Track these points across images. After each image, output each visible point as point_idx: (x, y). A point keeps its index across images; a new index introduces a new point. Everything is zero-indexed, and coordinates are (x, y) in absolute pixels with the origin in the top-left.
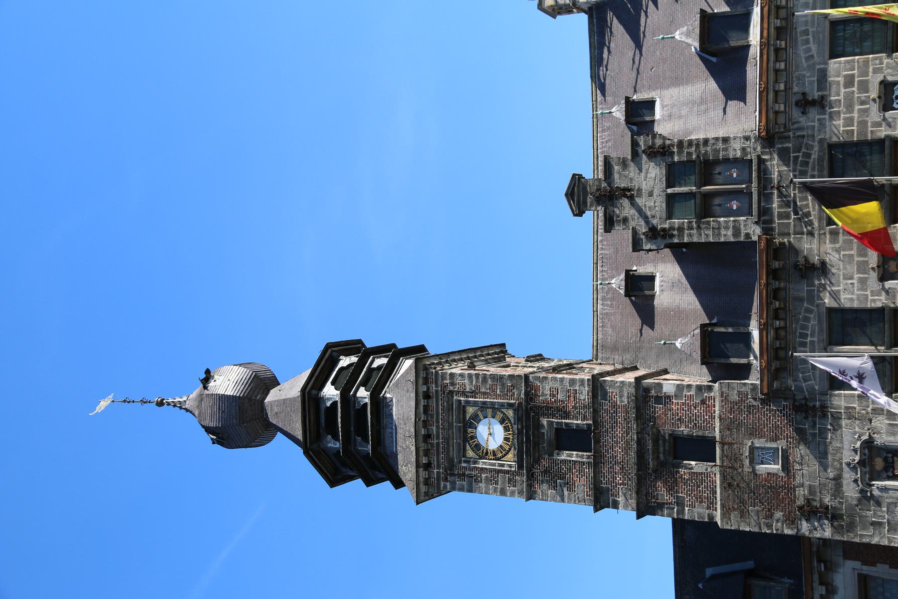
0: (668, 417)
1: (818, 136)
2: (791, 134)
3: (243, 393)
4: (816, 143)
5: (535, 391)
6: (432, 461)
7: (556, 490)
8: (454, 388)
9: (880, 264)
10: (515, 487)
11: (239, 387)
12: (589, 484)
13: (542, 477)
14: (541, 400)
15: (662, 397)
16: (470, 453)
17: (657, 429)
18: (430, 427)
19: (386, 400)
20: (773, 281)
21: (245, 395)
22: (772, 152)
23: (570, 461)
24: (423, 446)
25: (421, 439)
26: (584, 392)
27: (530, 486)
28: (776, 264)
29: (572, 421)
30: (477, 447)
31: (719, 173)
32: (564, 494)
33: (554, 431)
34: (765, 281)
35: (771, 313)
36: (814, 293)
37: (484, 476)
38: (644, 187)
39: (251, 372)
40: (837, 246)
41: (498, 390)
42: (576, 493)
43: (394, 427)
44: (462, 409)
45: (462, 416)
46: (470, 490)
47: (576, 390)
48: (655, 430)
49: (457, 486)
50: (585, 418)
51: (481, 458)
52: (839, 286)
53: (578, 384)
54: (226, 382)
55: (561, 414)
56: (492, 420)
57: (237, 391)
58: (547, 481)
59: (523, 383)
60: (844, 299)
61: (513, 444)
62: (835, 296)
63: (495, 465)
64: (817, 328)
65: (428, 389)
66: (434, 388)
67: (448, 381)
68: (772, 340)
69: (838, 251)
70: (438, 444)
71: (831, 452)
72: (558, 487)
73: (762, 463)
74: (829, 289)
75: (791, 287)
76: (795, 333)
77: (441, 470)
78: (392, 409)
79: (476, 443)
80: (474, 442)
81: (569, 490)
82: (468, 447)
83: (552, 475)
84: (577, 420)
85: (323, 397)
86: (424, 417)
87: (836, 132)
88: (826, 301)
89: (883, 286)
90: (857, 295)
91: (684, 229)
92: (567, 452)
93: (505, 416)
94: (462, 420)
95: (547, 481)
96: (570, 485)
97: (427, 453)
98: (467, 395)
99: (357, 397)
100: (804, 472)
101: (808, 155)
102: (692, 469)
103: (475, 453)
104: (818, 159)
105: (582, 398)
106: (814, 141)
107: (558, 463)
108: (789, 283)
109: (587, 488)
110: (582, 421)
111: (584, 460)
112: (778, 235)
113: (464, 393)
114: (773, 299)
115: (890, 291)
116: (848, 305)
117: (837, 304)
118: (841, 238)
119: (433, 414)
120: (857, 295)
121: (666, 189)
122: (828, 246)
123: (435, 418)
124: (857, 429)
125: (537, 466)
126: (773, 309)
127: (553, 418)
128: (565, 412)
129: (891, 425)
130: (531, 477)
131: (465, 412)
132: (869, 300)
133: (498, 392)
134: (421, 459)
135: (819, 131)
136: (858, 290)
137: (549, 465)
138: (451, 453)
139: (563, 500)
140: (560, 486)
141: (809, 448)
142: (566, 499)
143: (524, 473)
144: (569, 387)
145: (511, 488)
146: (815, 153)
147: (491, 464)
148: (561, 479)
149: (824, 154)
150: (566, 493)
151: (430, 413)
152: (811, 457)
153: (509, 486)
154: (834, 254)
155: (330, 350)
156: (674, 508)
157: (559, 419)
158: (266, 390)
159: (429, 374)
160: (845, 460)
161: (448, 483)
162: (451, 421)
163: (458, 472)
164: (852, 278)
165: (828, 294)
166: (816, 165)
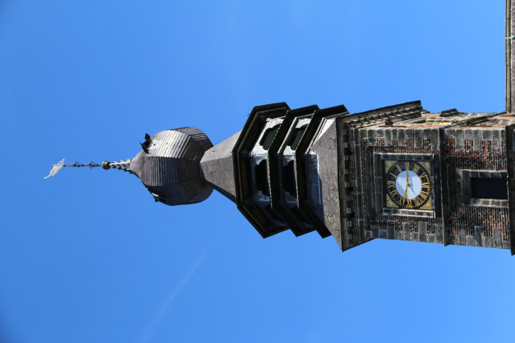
3: (180, 155)
5: (451, 144)
6: (355, 212)
7: (474, 235)
8: (373, 144)
10: (434, 233)
11: (177, 149)
12: (506, 229)
13: (459, 223)
14: (457, 152)
16: (391, 203)
18: (352, 181)
19: (310, 157)
21: (183, 156)
23: (486, 208)
24: (346, 198)
25: (344, 191)
26: (498, 142)
27: (448, 232)
29: (487, 171)
30: (397, 197)
32: (481, 239)
33: (470, 180)
37: (404, 224)
39: (187, 136)
41: (415, 144)
42: (493, 238)
43: (319, 182)
44: (381, 163)
45: (381, 170)
46: (392, 237)
47: (490, 141)
49: (379, 234)
50: (499, 167)
51: (400, 208)
53: (492, 136)
54: (164, 146)
55: (477, 165)
56: (410, 172)
57: (175, 153)
58: (465, 227)
59: (439, 137)
61: (431, 194)
65: (349, 145)
66: (354, 145)
67: (367, 138)
70: (360, 196)
72: (476, 232)
77: (364, 220)
78: (316, 165)
79: (395, 194)
80: (394, 193)
81: (486, 234)
82: (388, 198)
83: (469, 221)
84: (492, 170)
85: (253, 157)
86: (346, 172)
92: (483, 200)
93: (422, 169)
94: (381, 174)
96: (487, 230)
97: (350, 204)
98: (385, 150)
99: (283, 156)
103: (395, 203)
105: (497, 149)
107: (475, 210)
109: (503, 233)
110: (497, 170)
111: (500, 206)
113: (383, 149)
119: (355, 169)
123: (356, 172)
125: (454, 213)
127: (468, 169)
128: (480, 163)
130: (449, 224)
131: (384, 166)
133: (415, 146)
134: (344, 210)
137: (466, 212)
138: (373, 204)
139: (480, 245)
140: (478, 231)
142: (484, 243)
143: (442, 220)
144: (484, 138)
145: (430, 234)
147: (410, 213)
148: (478, 225)
150: (483, 238)
151: (352, 167)
153: (428, 233)
157: (475, 169)
158: (201, 152)
161: (371, 232)
162: (371, 174)
163: (380, 221)
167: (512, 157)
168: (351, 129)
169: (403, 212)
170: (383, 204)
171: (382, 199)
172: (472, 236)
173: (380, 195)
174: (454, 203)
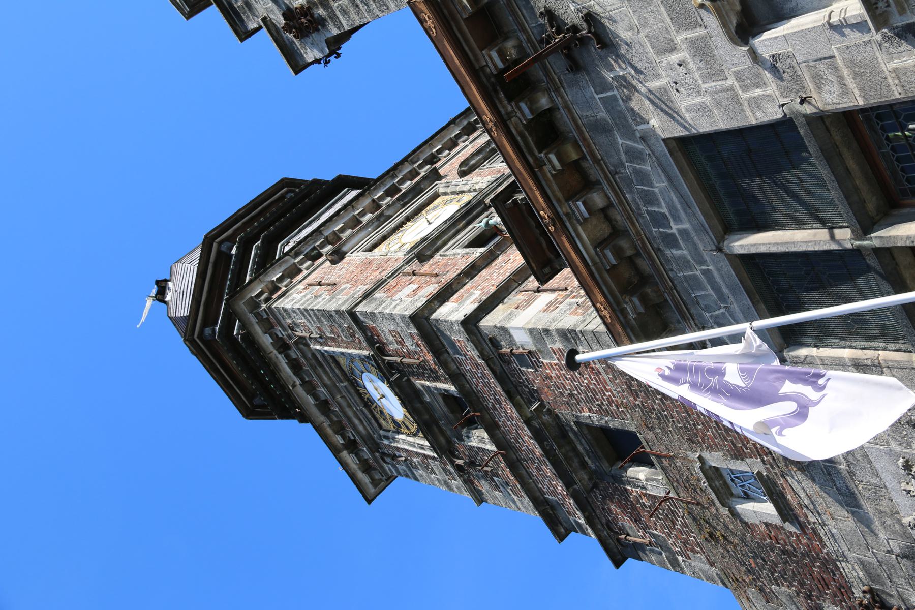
0: (554, 391)
5: (378, 337)
6: (352, 438)
15: (522, 355)
17: (550, 412)
20: (513, 104)
28: (493, 59)
34: (489, 116)
35: (555, 189)
36: (620, 106)
45: (337, 371)
48: (546, 418)
52: (658, 76)
60: (690, 109)
62: (664, 107)
63: (414, 446)
66: (283, 333)
68: (592, 251)
71: (866, 493)
73: (747, 497)
74: (643, 90)
75: (569, 98)
76: (640, 215)
88: (654, 122)
89: (754, 55)
90: (711, 94)
94: (342, 378)
95: (483, 477)
100: (834, 531)
102: (643, 488)
108: (557, 90)
114: (540, 152)
115: (779, 64)
116: (705, 126)
117: (680, 128)
120: (711, 94)
124: (894, 446)
132: (746, 104)
136: (705, 79)
138: (361, 428)
141: (813, 480)
150: (516, 498)
152: (829, 500)
155: (215, 245)
156: (661, 554)
159: (261, 314)
164: (672, 49)
165: (647, 102)
167: (457, 367)
168: (263, 308)
170: (376, 425)
171: (370, 416)
172: (500, 493)
173: (362, 411)
174: (442, 440)
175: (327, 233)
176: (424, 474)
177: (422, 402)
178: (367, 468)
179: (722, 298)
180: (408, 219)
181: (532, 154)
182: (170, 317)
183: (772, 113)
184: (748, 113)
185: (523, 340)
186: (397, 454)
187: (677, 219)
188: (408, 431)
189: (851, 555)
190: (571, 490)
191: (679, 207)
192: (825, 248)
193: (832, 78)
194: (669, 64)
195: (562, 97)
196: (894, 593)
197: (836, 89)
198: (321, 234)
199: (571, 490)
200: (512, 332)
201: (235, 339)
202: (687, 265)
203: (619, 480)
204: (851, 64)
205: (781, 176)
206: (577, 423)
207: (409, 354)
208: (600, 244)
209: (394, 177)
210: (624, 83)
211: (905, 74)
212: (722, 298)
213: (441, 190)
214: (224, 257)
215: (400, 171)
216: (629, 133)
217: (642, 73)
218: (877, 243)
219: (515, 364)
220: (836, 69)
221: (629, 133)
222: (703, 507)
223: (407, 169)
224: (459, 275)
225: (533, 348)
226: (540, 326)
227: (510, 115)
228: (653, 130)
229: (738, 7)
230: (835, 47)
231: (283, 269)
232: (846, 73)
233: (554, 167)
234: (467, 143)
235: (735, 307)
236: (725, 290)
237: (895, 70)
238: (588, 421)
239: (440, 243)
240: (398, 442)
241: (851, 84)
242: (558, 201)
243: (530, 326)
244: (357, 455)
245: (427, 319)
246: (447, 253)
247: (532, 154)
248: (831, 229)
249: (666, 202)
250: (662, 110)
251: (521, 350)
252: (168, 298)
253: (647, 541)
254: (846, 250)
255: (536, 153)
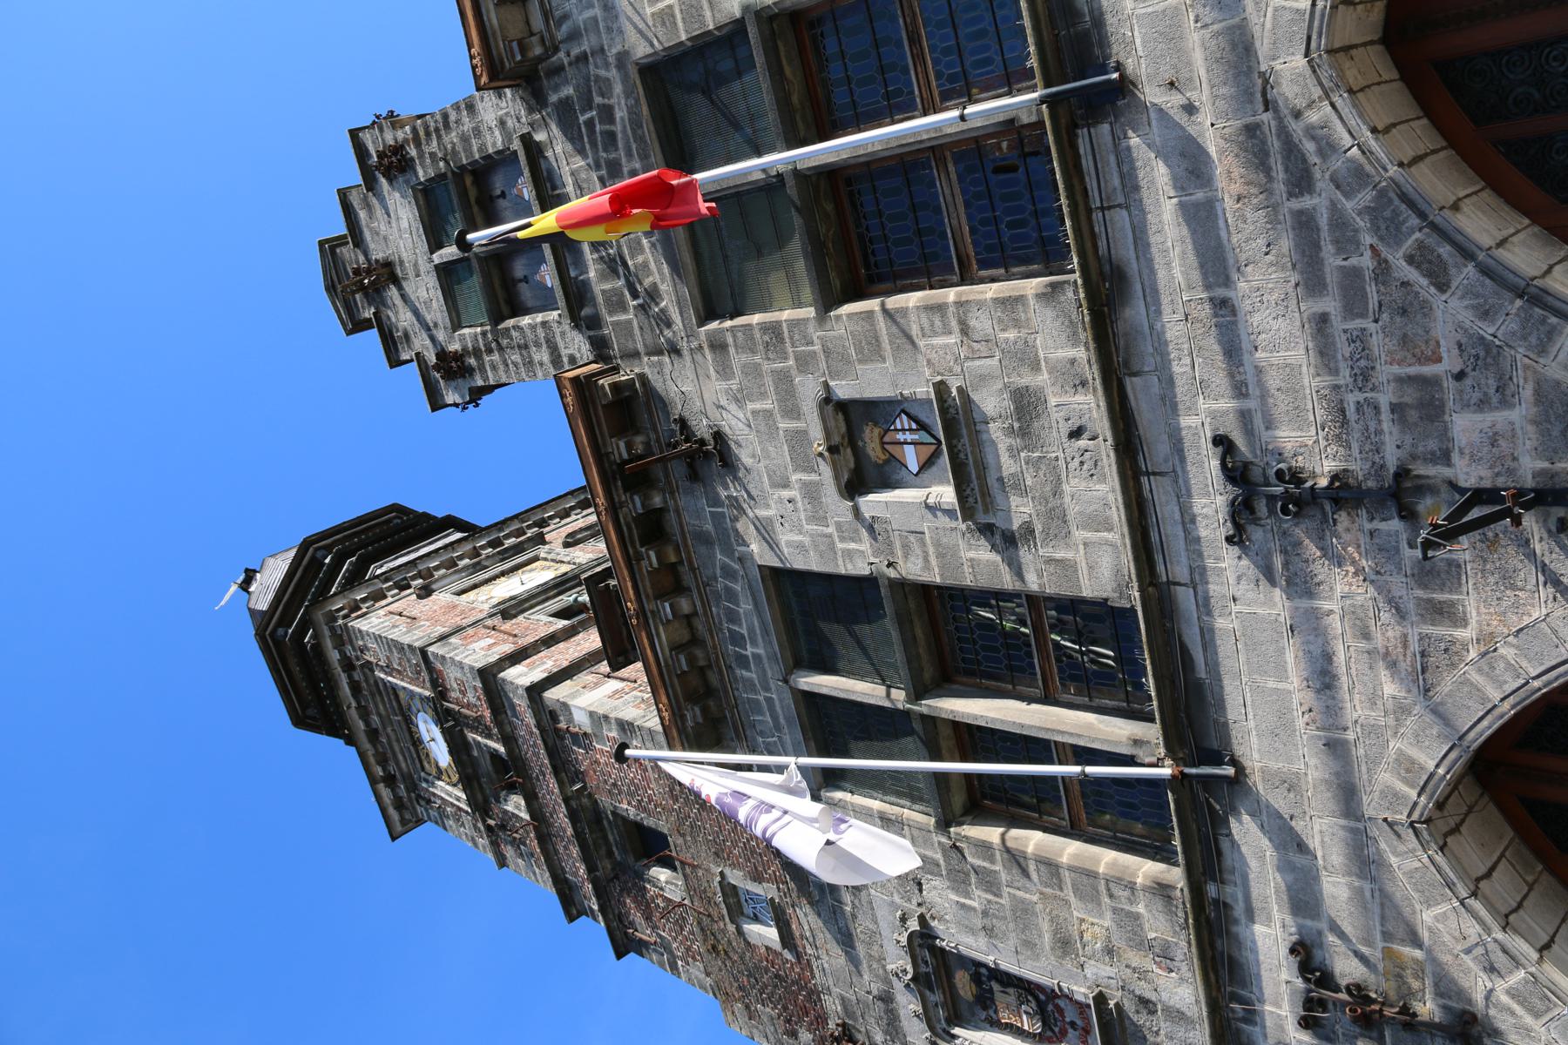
1: (610, 46)
2: (562, 54)
4: (613, 74)
9: (836, 440)
17: (590, 796)
20: (628, 495)
22: (548, 120)
28: (619, 449)
31: (503, 195)
38: (404, 255)
40: (734, 384)
45: (394, 704)
48: (585, 801)
52: (768, 506)
60: (789, 544)
62: (767, 536)
63: (451, 796)
64: (756, 623)
69: (739, 401)
71: (862, 937)
73: (756, 919)
74: (751, 514)
75: (681, 503)
76: (721, 630)
87: (641, 25)
89: (856, 511)
90: (811, 536)
91: (480, 350)
94: (398, 712)
100: (826, 966)
101: (607, 113)
102: (661, 889)
104: (629, 119)
106: (607, 66)
108: (672, 493)
112: (621, 357)
114: (642, 547)
116: (799, 564)
118: (737, 359)
120: (811, 536)
121: (432, 253)
122: (715, 389)
124: (897, 899)
126: (648, 571)
129: (963, 906)
132: (840, 553)
135: (609, 30)
138: (403, 765)
141: (819, 915)
146: (619, 104)
149: (637, 100)
150: (537, 871)
152: (829, 936)
154: (733, 407)
155: (311, 550)
156: (663, 955)
160: (890, 967)
162: (383, 713)
164: (786, 485)
166: (632, 140)
169: (443, 789)
174: (479, 797)
175: (421, 567)
176: (454, 826)
177: (470, 755)
178: (399, 805)
179: (778, 727)
180: (503, 574)
181: (634, 547)
182: (249, 609)
183: (862, 569)
184: (840, 562)
185: (581, 720)
186: (433, 799)
187: (754, 643)
188: (447, 779)
189: (836, 990)
190: (592, 875)
191: (758, 632)
192: (880, 704)
193: (918, 551)
194: (780, 498)
195: (676, 501)
196: (863, 1029)
197: (920, 562)
198: (416, 565)
199: (592, 875)
200: (573, 710)
201: (304, 646)
202: (750, 685)
203: (640, 876)
204: (937, 544)
205: (856, 628)
206: (614, 813)
207: (468, 706)
208: (676, 648)
209: (501, 530)
210: (735, 503)
211: (979, 565)
212: (778, 727)
213: (543, 555)
214: (316, 563)
215: (508, 527)
216: (729, 551)
217: (753, 499)
218: (925, 710)
219: (568, 742)
220: (923, 544)
221: (729, 551)
222: (713, 920)
223: (515, 526)
224: (537, 641)
225: (589, 731)
226: (601, 711)
227: (622, 505)
228: (751, 554)
229: (852, 465)
230: (927, 525)
231: (369, 590)
232: (931, 550)
233: (651, 565)
234: (579, 516)
235: (787, 738)
236: (782, 721)
237: (971, 560)
238: (624, 814)
239: (527, 605)
240: (436, 788)
241: (933, 561)
242: (647, 596)
243: (592, 709)
244: (393, 790)
245: (495, 676)
246: (532, 617)
247: (634, 547)
248: (889, 687)
249: (747, 625)
250: (764, 538)
251: (577, 729)
252: (252, 589)
253: (652, 940)
254: (898, 710)
255: (638, 546)
